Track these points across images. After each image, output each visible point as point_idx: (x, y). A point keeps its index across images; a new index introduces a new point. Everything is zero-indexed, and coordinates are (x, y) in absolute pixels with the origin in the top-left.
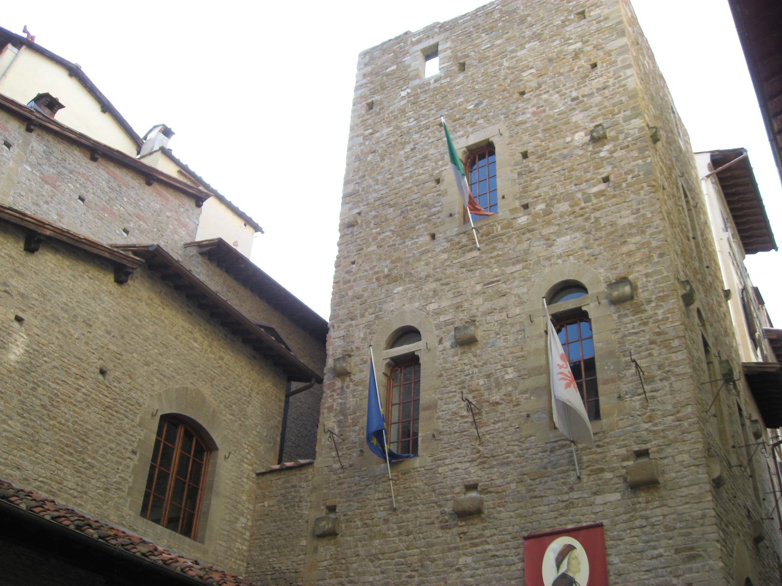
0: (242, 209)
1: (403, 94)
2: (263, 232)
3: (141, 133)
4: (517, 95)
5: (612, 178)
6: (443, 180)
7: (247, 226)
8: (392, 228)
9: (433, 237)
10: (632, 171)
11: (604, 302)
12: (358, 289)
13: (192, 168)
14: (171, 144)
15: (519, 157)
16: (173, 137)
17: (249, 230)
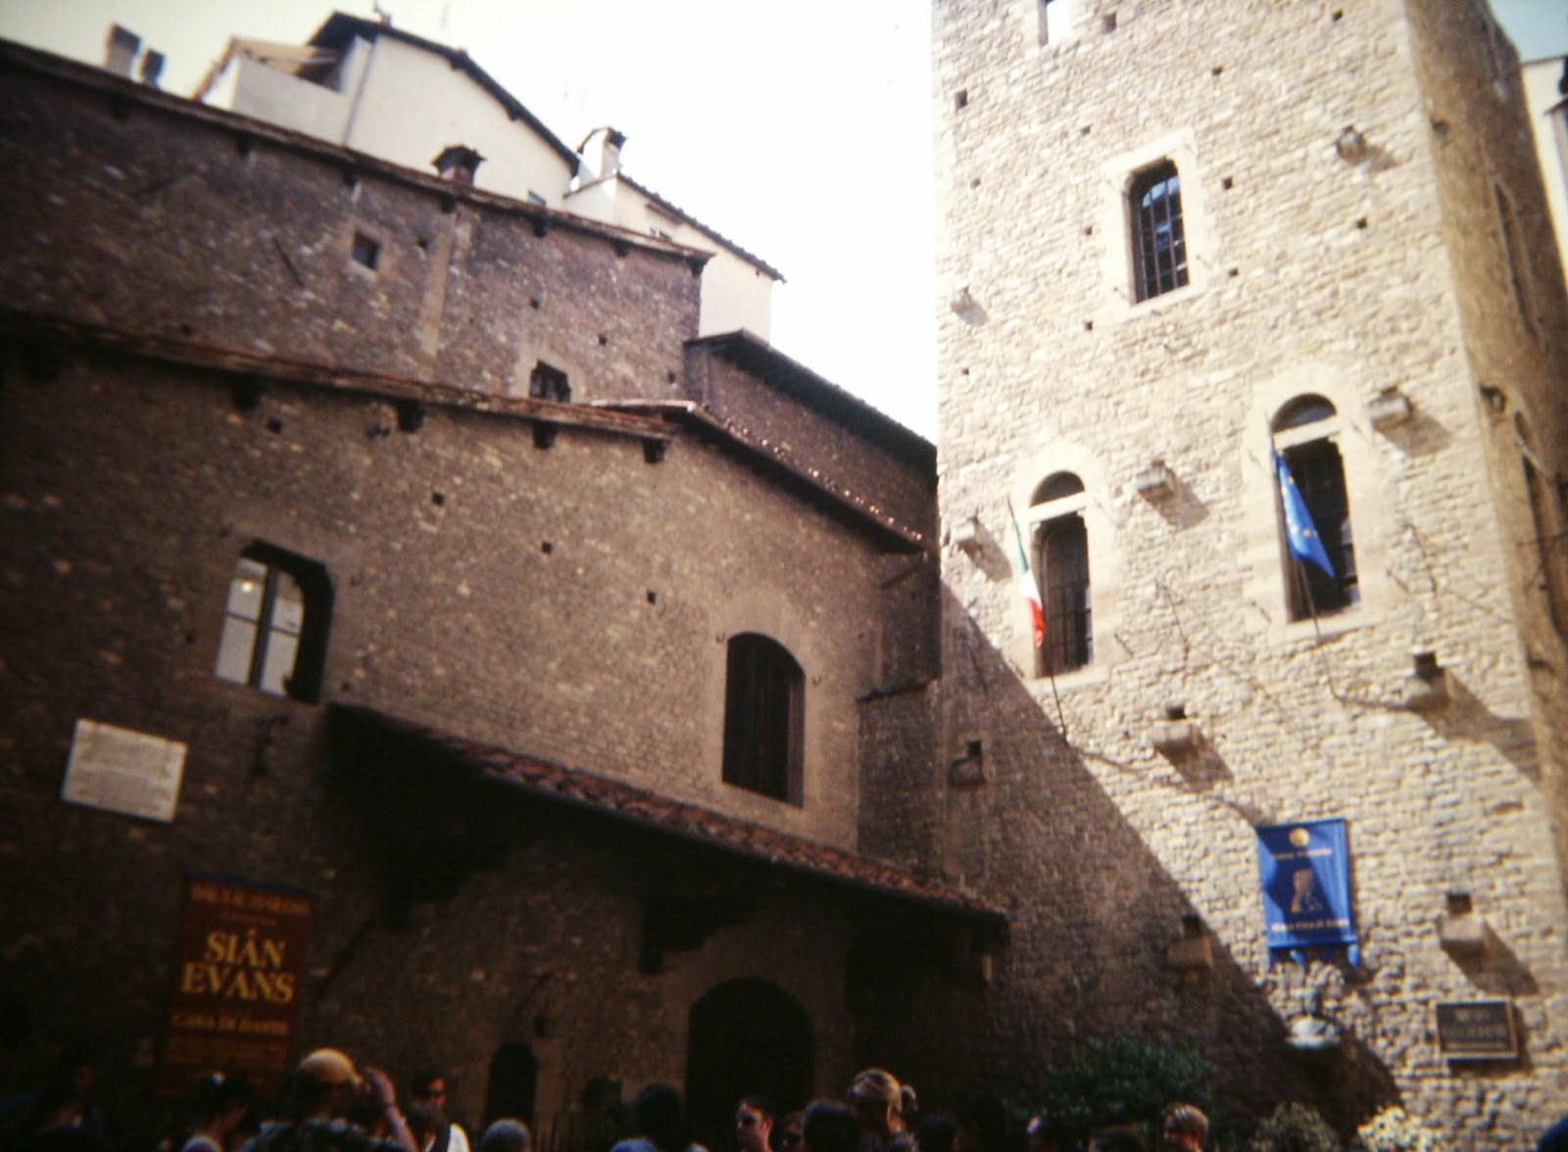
0: (749, 250)
1: (1016, 74)
2: (784, 281)
3: (571, 143)
4: (1208, 75)
5: (1371, 221)
6: (1099, 231)
7: (762, 276)
8: (1022, 311)
9: (1089, 326)
10: (1405, 205)
11: (1366, 427)
12: (980, 408)
13: (665, 197)
14: (630, 161)
15: (1219, 185)
16: (625, 146)
17: (764, 279)
